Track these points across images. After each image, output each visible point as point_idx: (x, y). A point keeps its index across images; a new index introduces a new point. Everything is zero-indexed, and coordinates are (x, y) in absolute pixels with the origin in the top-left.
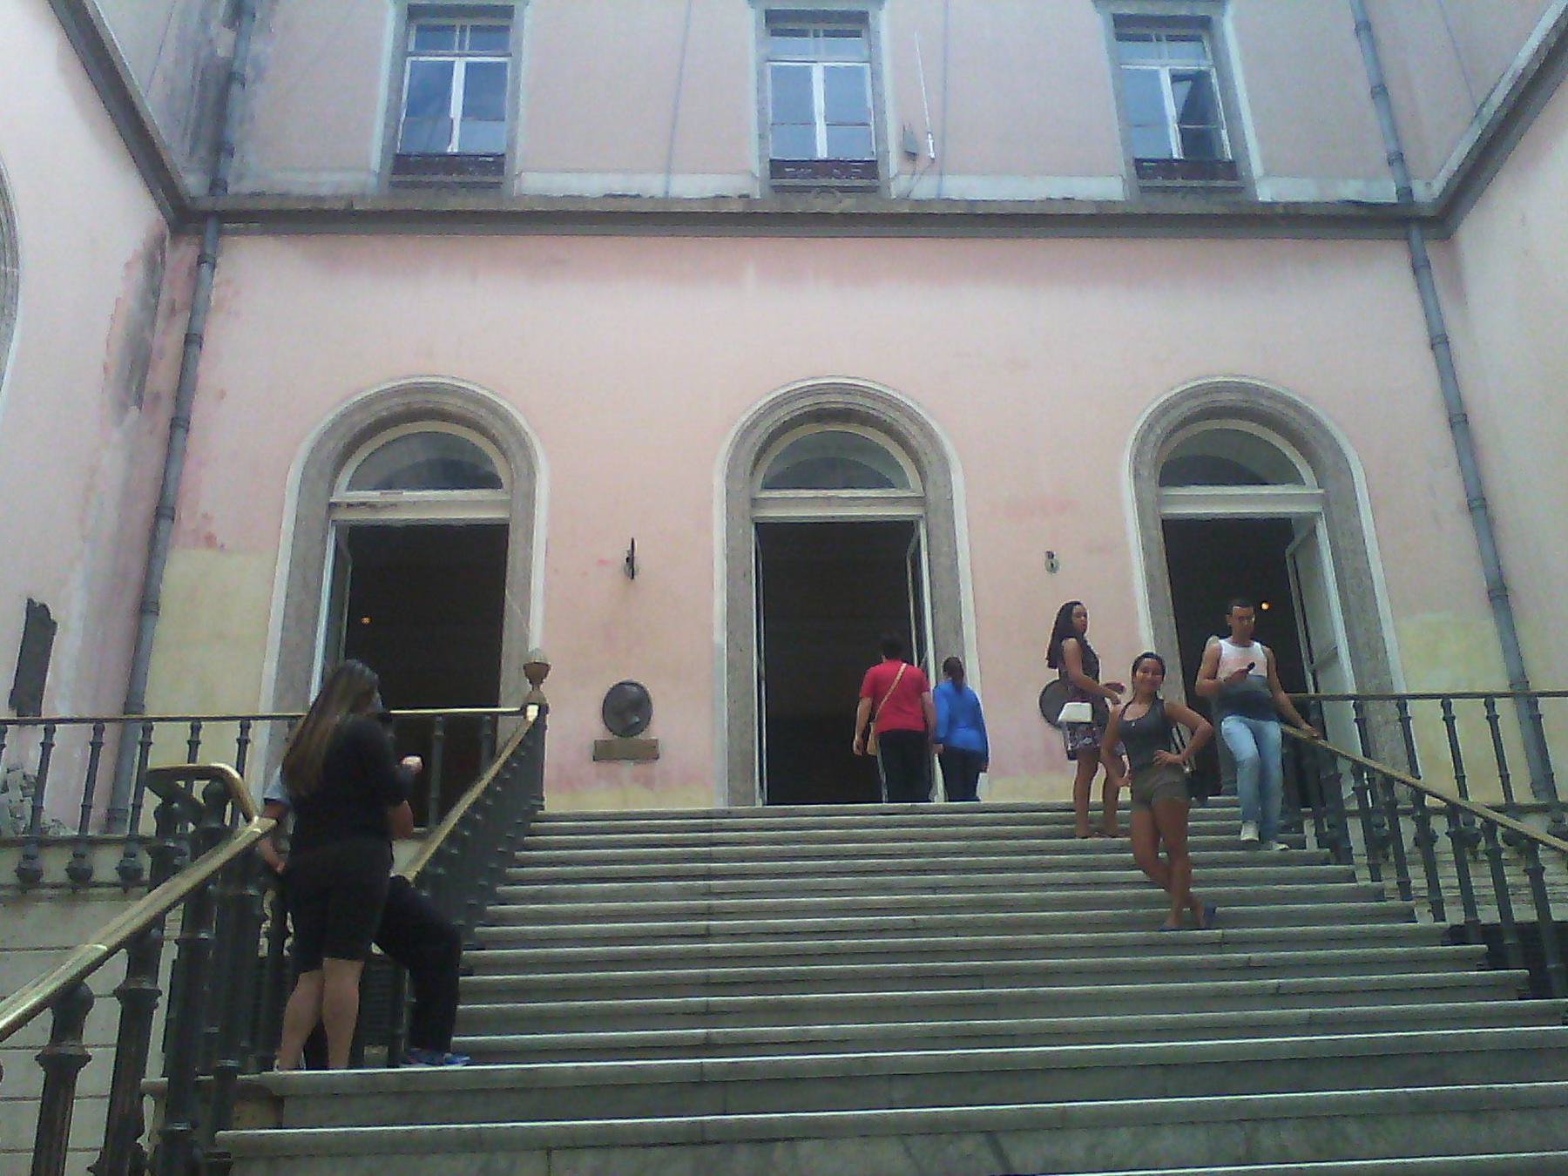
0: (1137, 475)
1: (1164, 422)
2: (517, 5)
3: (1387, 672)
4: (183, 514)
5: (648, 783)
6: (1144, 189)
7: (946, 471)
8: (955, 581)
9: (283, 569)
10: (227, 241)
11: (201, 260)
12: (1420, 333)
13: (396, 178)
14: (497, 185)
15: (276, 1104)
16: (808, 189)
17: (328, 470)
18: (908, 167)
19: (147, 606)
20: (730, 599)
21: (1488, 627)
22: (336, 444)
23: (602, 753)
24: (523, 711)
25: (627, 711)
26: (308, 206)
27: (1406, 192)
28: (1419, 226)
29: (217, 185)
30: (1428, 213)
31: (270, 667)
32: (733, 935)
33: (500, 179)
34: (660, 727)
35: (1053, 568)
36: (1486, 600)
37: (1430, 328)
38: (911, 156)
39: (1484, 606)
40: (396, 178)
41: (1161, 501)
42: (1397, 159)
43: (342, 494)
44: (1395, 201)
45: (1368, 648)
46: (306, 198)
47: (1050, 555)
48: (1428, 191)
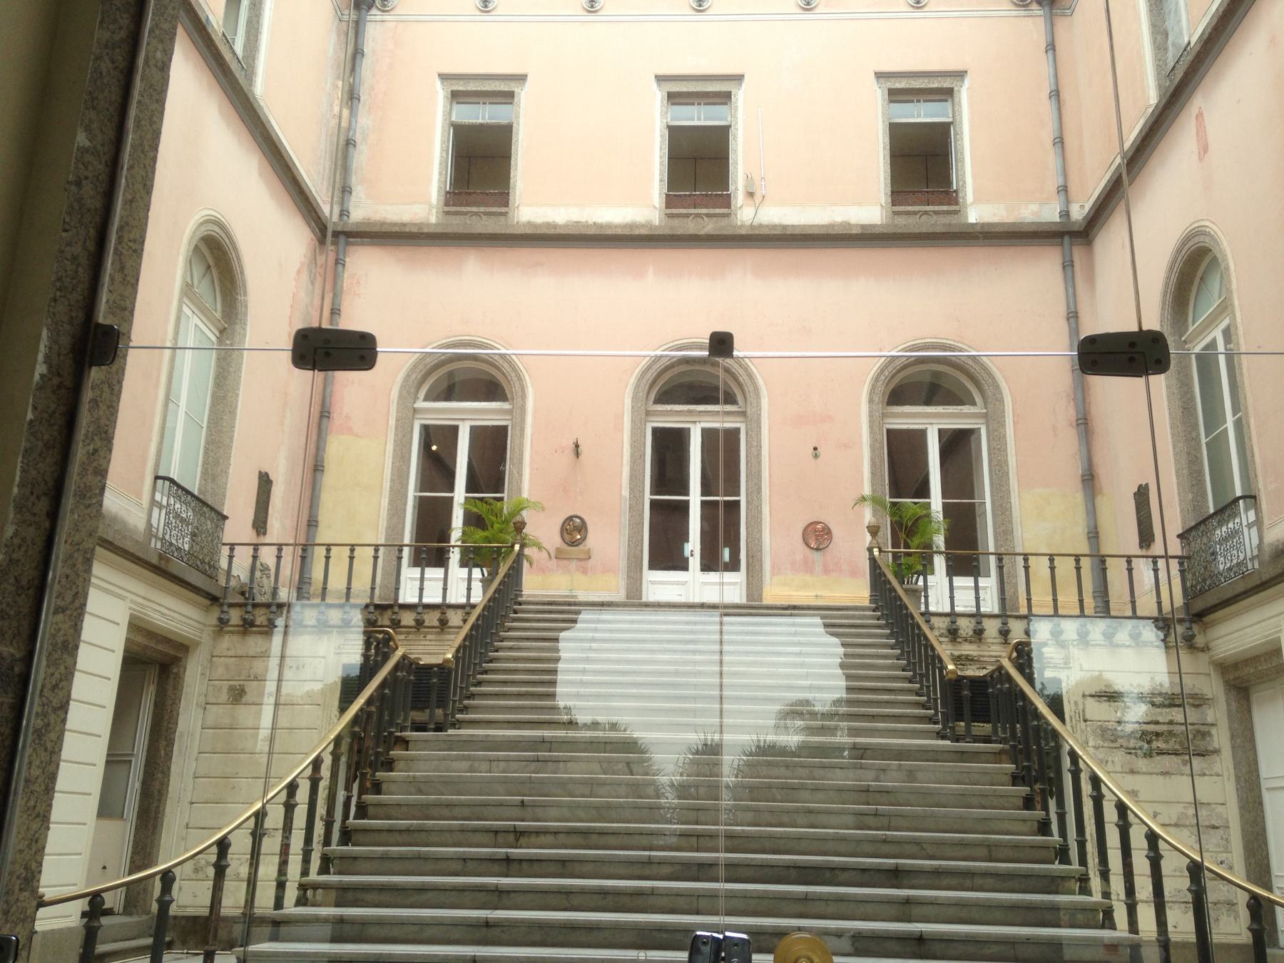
0: (871, 401)
1: (890, 369)
2: (516, 90)
3: (1011, 522)
4: (335, 415)
5: (585, 572)
6: (895, 213)
7: (758, 396)
8: (759, 463)
9: (390, 447)
10: (351, 249)
11: (337, 262)
12: (1062, 310)
13: (447, 209)
14: (505, 214)
15: (405, 743)
16: (687, 216)
17: (413, 390)
18: (750, 201)
19: (317, 468)
20: (632, 470)
21: (1079, 497)
22: (416, 376)
23: (560, 555)
24: (513, 546)
25: (574, 530)
26: (397, 229)
27: (1065, 214)
28: (1074, 237)
29: (344, 213)
30: (1076, 228)
31: (385, 502)
32: (596, 672)
33: (503, 210)
34: (594, 539)
35: (816, 456)
36: (1079, 479)
37: (1068, 307)
38: (751, 195)
39: (1080, 486)
40: (447, 209)
41: (884, 416)
42: (1064, 190)
43: (421, 404)
44: (1057, 219)
45: (1003, 509)
46: (395, 224)
47: (815, 449)
48: (1079, 212)
